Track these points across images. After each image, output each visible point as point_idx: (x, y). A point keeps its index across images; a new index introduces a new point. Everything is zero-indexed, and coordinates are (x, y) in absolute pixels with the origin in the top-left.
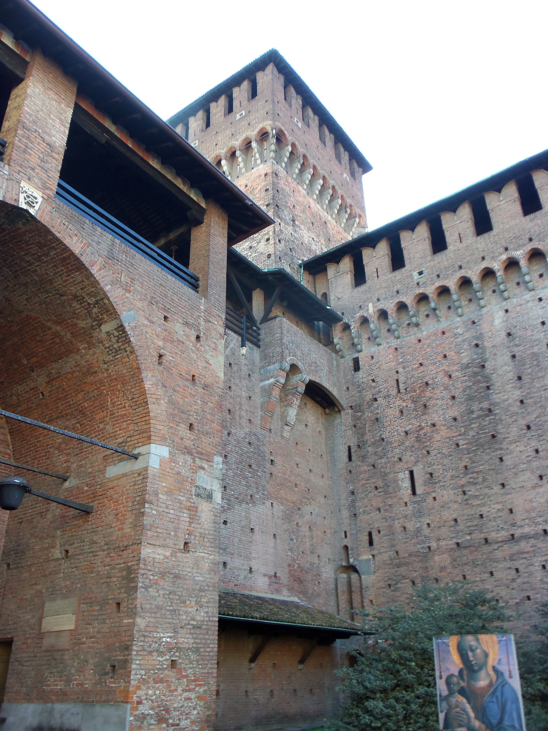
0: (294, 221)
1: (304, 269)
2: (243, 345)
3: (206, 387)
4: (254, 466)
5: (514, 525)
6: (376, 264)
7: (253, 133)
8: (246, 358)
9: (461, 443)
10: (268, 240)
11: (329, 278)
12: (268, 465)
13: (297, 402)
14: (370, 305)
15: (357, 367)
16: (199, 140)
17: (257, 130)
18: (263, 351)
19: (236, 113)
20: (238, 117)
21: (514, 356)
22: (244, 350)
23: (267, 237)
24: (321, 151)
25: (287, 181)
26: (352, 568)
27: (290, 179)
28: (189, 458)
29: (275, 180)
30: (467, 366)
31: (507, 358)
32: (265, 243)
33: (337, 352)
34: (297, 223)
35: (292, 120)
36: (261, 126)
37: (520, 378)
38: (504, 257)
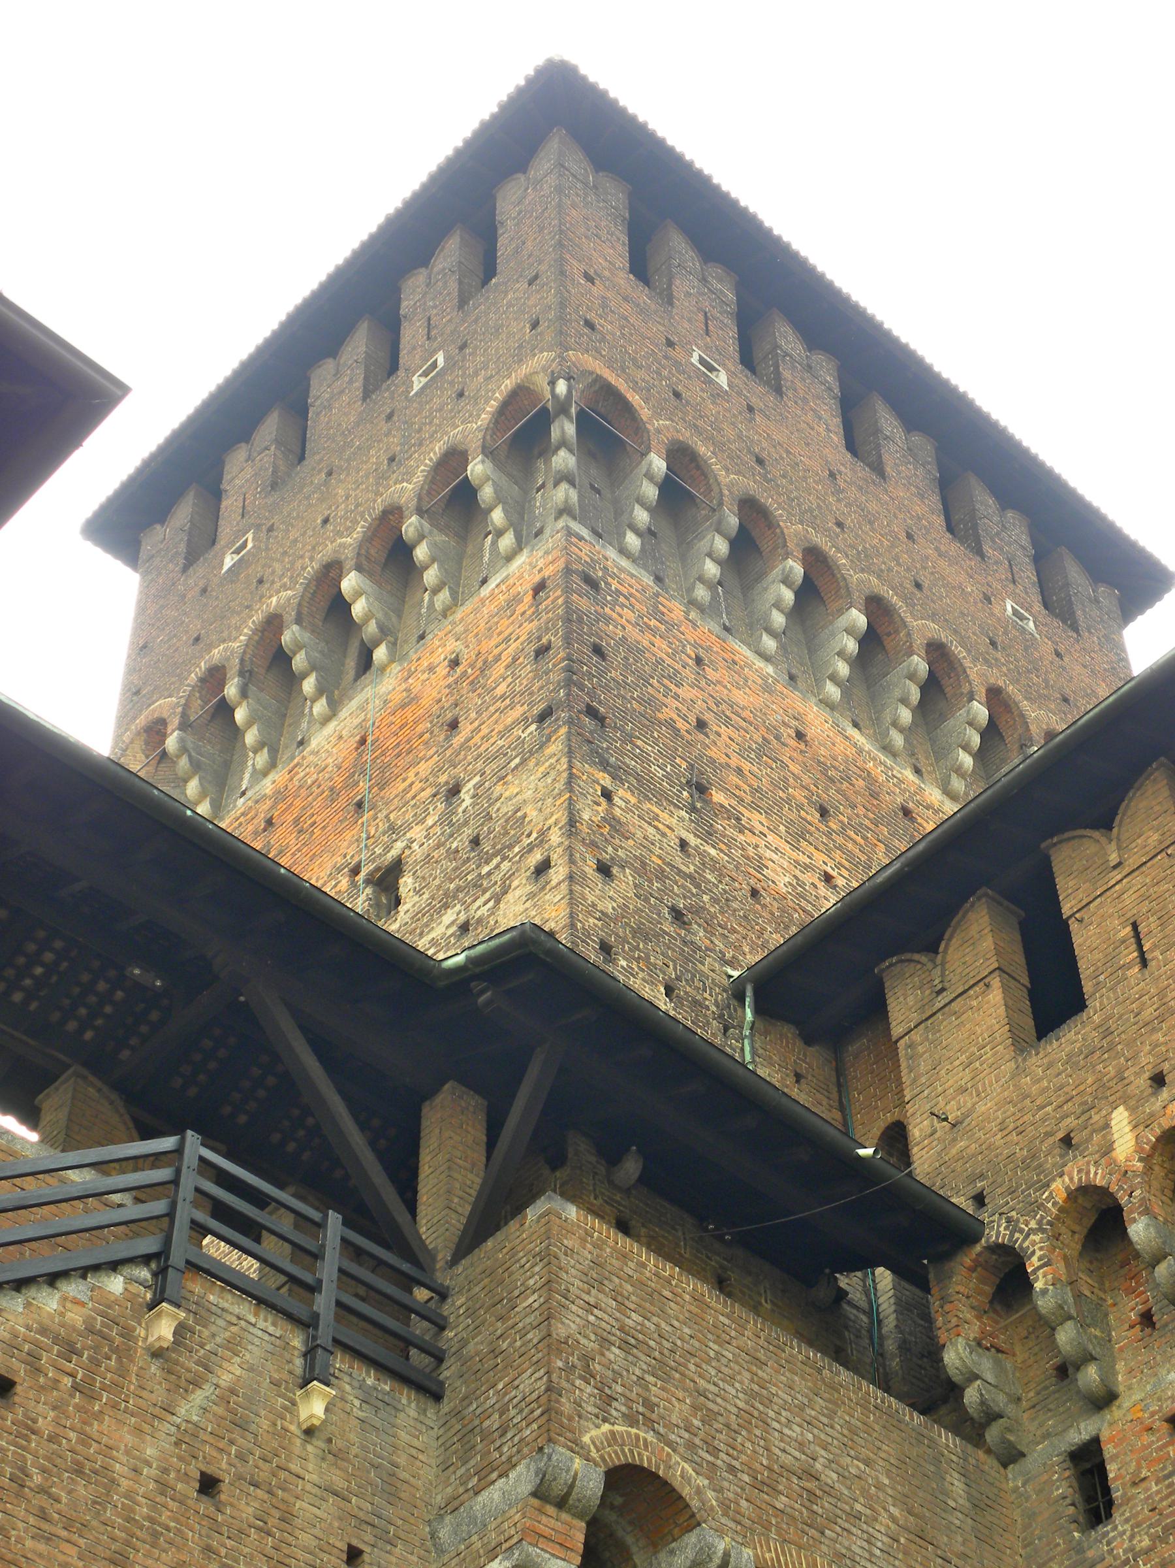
1: (757, 1011)
2: (313, 1372)
6: (1129, 898)
7: (472, 426)
8: (336, 1455)
10: (543, 868)
11: (897, 1030)
14: (1120, 1119)
16: (258, 527)
18: (457, 1413)
19: (410, 372)
20: (418, 382)
22: (315, 1406)
23: (537, 857)
24: (853, 493)
25: (657, 614)
27: (676, 610)
29: (583, 603)
32: (529, 888)
33: (972, 1429)
34: (718, 797)
35: (678, 354)
36: (508, 384)
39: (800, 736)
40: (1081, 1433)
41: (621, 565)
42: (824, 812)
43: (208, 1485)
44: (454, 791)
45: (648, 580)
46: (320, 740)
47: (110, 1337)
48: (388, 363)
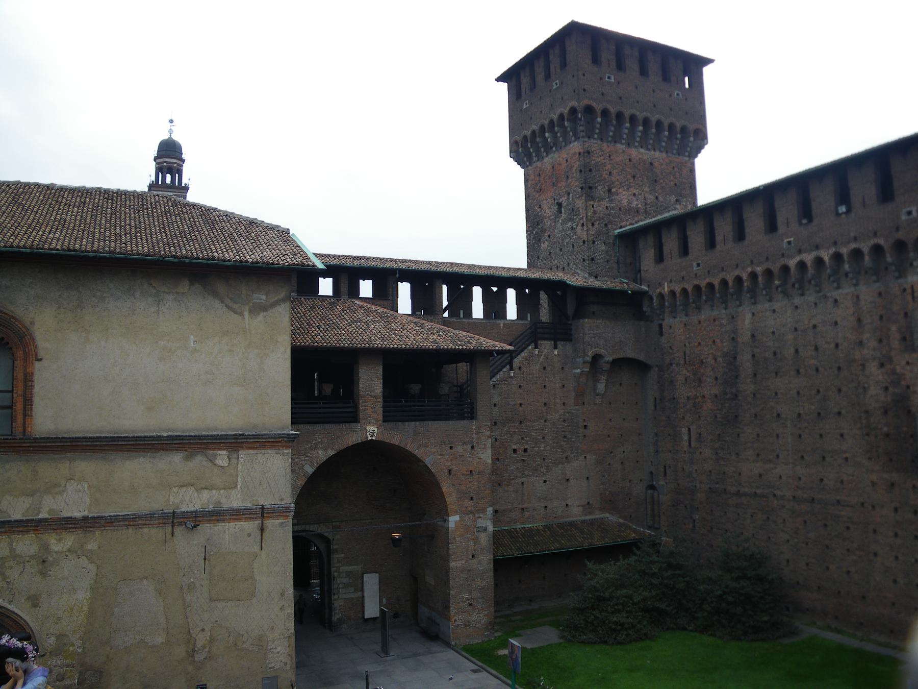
0: (609, 191)
2: (555, 348)
3: (480, 473)
4: (569, 436)
5: (740, 484)
9: (719, 416)
12: (581, 430)
13: (603, 378)
15: (661, 334)
17: (568, 109)
21: (753, 356)
26: (652, 487)
28: (471, 516)
29: (587, 160)
30: (725, 355)
31: (750, 357)
34: (614, 190)
37: (755, 375)
38: (749, 269)
39: (630, 160)
40: (660, 322)
41: (594, 144)
42: (634, 177)
43: (544, 368)
44: (569, 194)
45: (599, 142)
46: (546, 160)
47: (531, 355)
48: (548, 76)
